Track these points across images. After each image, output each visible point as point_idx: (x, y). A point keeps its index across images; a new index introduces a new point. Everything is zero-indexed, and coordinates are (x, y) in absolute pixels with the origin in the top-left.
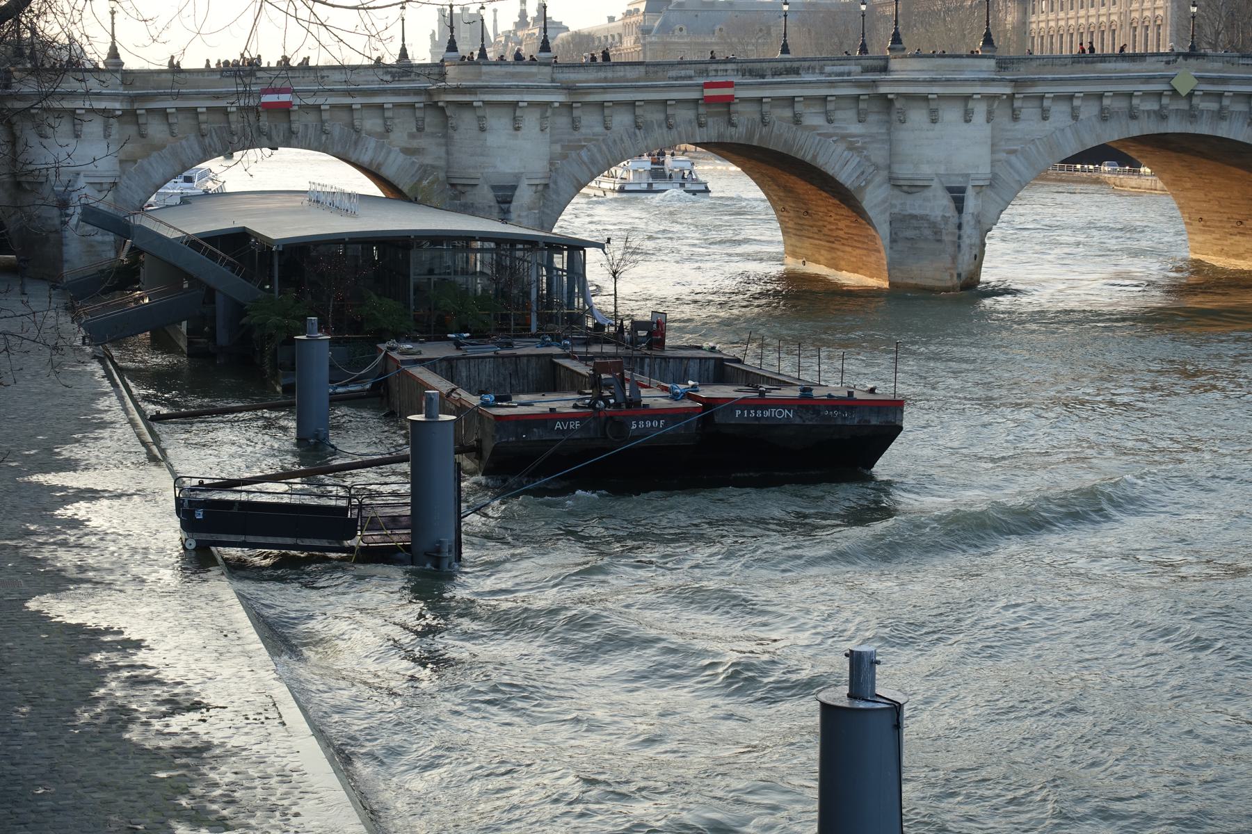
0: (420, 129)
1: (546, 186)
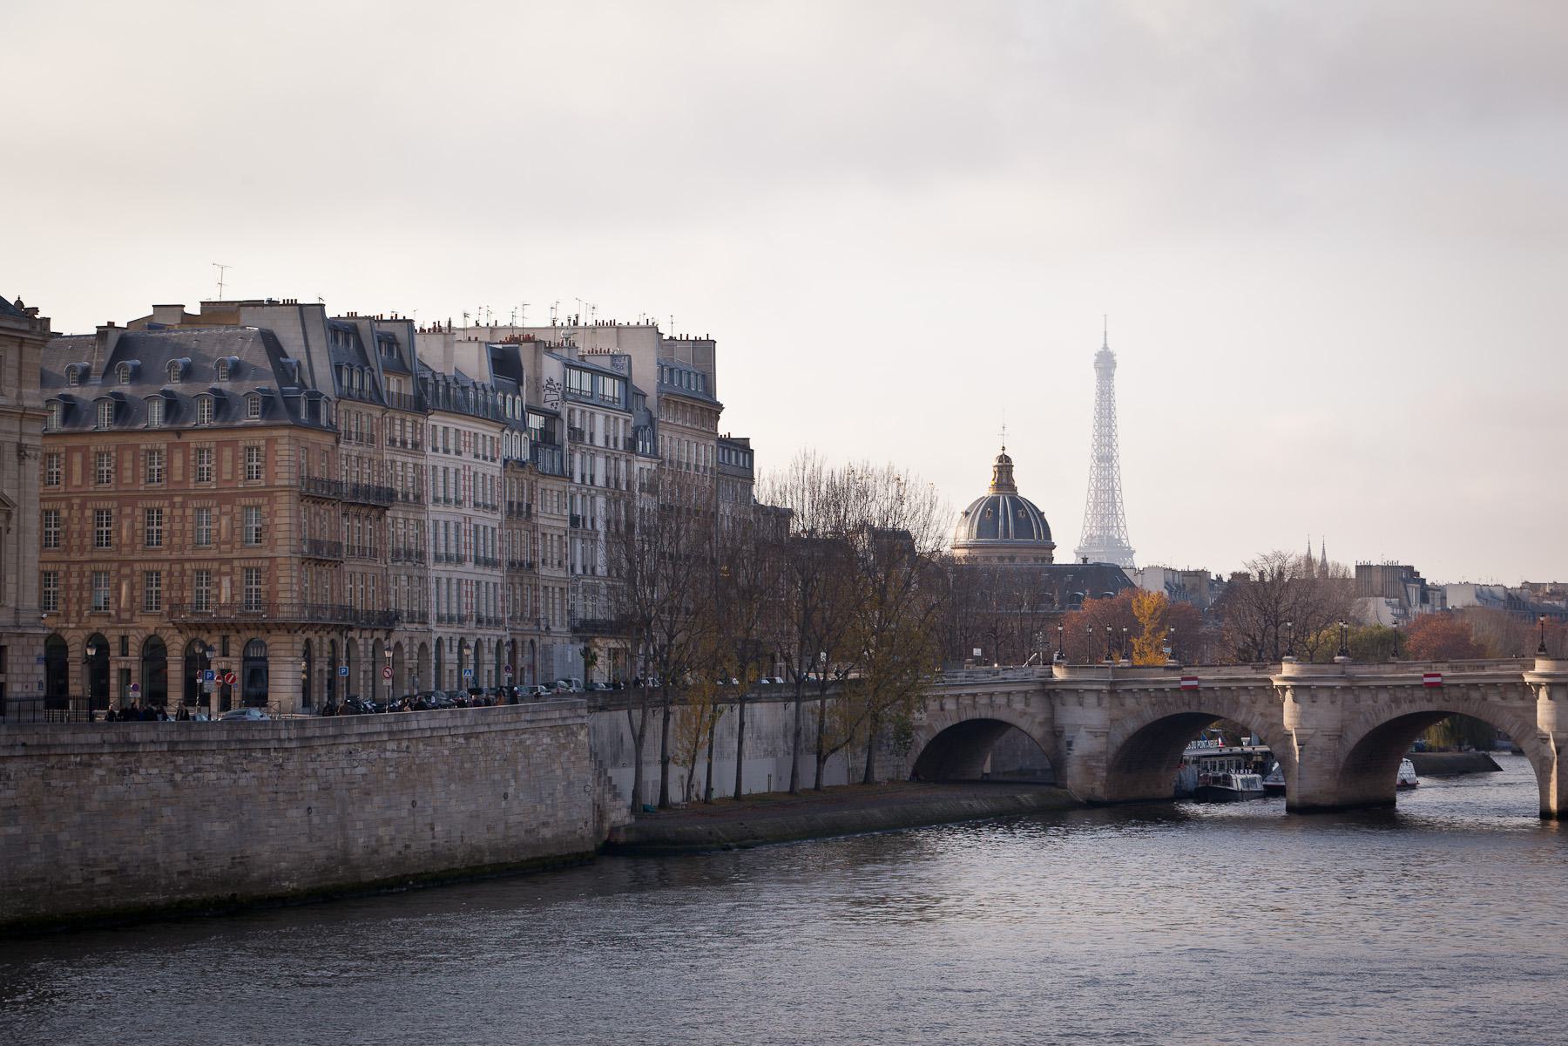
0: (1271, 702)
1: (1340, 736)
